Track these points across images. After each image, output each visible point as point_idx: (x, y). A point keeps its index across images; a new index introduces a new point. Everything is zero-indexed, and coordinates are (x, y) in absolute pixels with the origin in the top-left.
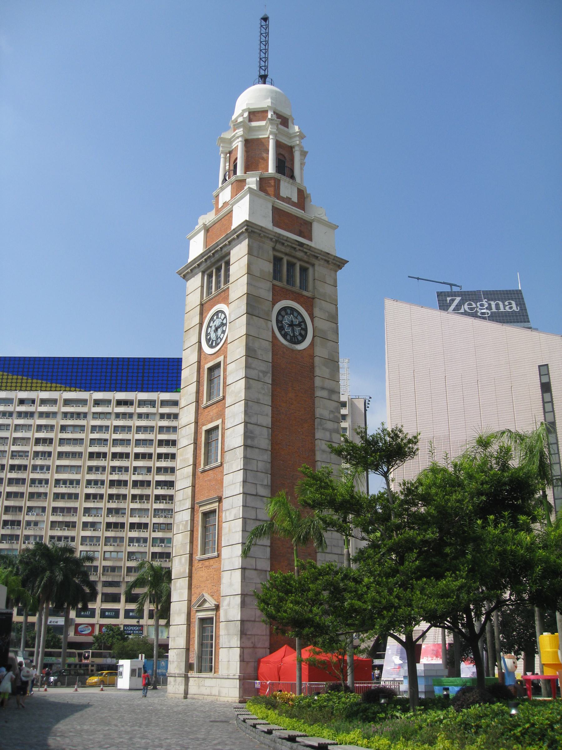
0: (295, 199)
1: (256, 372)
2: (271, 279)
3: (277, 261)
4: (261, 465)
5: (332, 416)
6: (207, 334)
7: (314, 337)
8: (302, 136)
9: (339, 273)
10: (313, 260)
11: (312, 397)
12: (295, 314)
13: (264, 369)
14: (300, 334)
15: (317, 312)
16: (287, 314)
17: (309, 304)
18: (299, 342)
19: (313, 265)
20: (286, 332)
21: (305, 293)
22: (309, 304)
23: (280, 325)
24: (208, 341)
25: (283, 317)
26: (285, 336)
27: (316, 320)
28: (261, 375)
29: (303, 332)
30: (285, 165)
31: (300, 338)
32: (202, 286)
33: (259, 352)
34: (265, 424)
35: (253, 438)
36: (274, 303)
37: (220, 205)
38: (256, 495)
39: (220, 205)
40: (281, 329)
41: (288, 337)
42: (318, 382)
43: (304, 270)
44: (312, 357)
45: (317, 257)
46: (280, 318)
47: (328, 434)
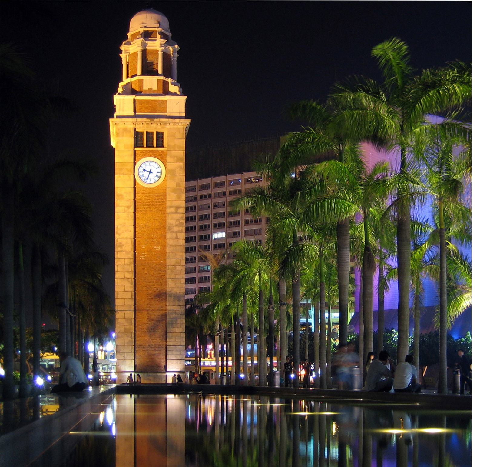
0: (155, 88)
1: (123, 208)
4: (127, 261)
5: (178, 223)
11: (164, 213)
12: (153, 164)
13: (128, 205)
15: (168, 159)
28: (126, 209)
29: (159, 174)
31: (157, 178)
33: (125, 195)
34: (129, 237)
35: (121, 247)
38: (124, 278)
42: (168, 204)
44: (165, 188)
47: (174, 235)
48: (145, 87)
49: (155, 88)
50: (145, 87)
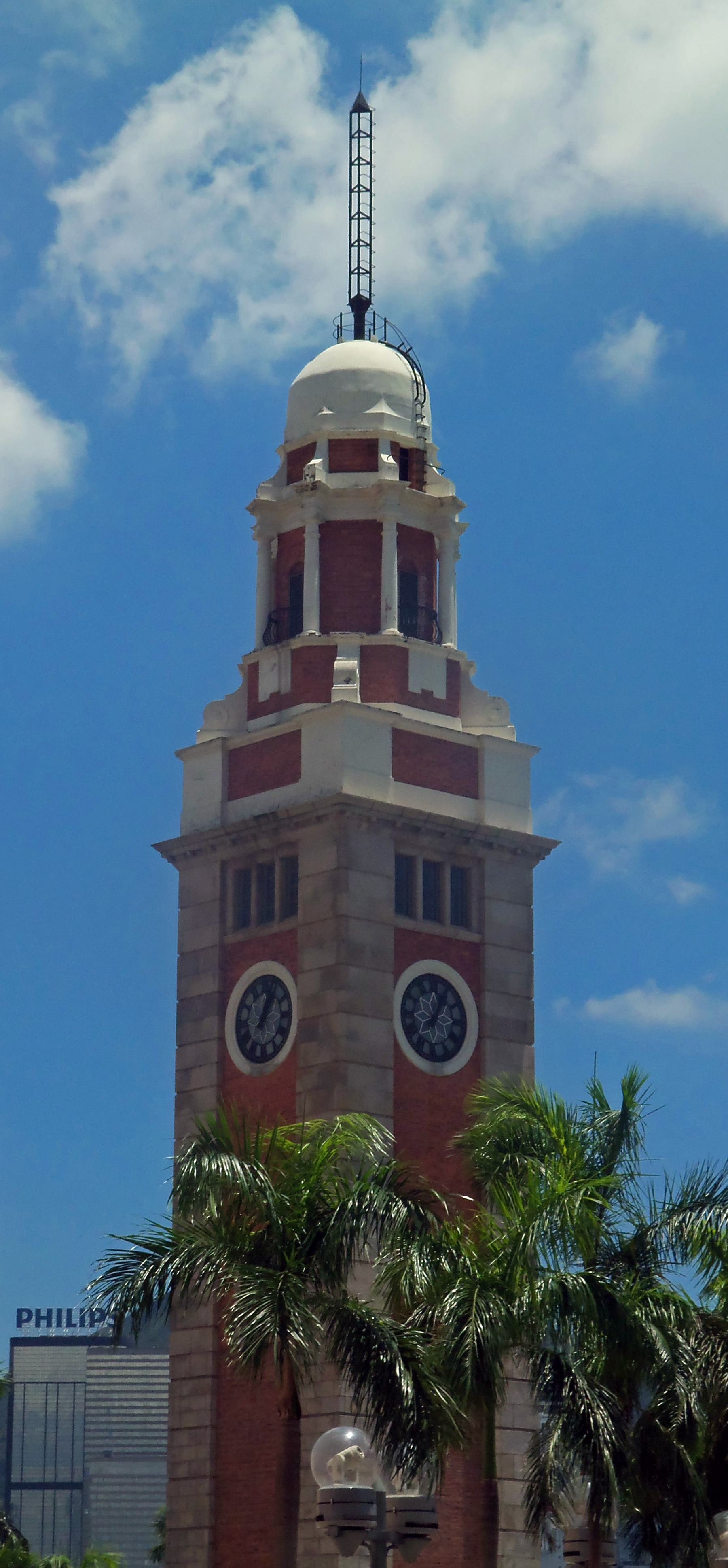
0: (440, 693)
2: (388, 911)
3: (404, 864)
6: (240, 1024)
7: (480, 1038)
8: (461, 528)
9: (540, 870)
10: (482, 852)
14: (451, 1036)
16: (423, 992)
17: (471, 961)
18: (449, 1055)
19: (480, 861)
20: (420, 1038)
21: (464, 935)
22: (471, 961)
23: (409, 1021)
24: (242, 1039)
25: (416, 1001)
26: (418, 1047)
27: (488, 996)
30: (422, 618)
32: (223, 899)
36: (397, 974)
37: (263, 695)
39: (263, 695)
40: (410, 1030)
41: (426, 1049)
43: (460, 876)
45: (490, 846)
46: (410, 1005)
48: (415, 686)
49: (440, 693)
50: (415, 686)
